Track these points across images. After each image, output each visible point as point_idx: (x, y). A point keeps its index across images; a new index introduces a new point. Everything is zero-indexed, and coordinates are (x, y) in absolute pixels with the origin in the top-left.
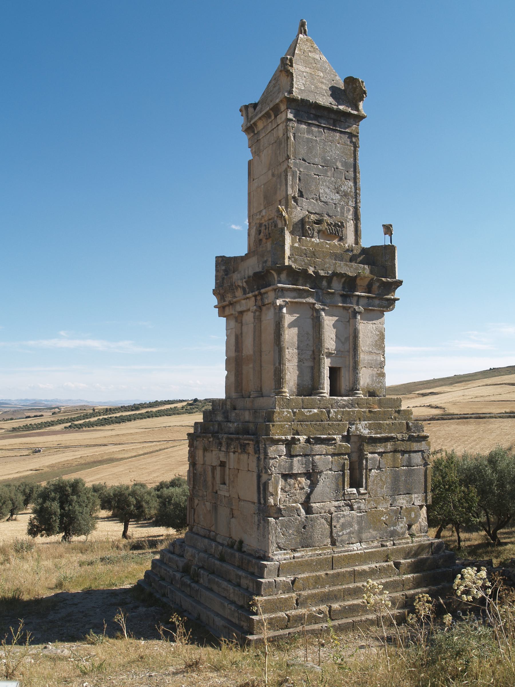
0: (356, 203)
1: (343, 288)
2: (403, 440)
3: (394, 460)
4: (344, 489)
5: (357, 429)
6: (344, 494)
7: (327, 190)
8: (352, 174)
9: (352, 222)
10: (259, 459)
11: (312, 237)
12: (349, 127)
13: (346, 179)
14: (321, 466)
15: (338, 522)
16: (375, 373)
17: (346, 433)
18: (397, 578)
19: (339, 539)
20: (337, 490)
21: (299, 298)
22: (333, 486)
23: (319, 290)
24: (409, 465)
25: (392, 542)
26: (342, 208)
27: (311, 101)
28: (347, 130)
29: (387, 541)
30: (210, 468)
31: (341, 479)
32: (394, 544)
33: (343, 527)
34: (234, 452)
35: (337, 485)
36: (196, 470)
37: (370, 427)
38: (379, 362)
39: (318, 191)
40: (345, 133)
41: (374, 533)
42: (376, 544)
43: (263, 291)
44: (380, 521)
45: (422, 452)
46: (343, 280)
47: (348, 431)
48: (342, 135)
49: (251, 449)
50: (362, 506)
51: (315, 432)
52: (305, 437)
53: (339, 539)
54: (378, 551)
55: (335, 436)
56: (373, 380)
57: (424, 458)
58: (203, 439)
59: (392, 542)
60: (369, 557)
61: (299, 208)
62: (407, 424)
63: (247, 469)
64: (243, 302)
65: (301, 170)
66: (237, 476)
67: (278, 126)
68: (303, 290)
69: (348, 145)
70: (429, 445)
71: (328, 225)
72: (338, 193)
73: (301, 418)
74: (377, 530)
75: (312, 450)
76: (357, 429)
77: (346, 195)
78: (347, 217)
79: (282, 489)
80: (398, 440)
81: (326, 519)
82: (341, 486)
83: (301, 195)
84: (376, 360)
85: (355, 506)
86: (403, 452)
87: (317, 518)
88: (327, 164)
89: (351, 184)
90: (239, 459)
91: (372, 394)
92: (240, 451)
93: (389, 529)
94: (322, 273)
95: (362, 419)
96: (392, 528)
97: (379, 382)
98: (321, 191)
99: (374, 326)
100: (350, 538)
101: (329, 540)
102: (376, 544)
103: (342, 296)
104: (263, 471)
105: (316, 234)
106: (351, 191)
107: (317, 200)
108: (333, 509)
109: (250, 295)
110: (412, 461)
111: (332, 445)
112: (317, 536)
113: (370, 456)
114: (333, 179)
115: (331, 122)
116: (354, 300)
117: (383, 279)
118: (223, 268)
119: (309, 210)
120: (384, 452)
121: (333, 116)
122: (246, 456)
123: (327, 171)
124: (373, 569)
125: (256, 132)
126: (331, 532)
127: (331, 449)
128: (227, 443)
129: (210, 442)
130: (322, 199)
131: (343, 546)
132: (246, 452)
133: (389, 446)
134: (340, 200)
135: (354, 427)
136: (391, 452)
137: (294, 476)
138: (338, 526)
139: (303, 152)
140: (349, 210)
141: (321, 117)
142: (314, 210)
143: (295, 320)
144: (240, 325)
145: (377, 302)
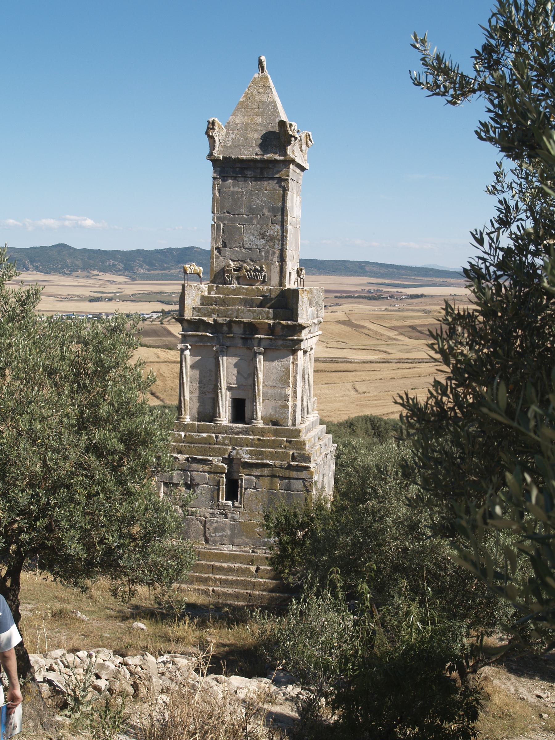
0: (282, 245)
1: (245, 332)
2: (281, 468)
3: (272, 483)
4: (218, 501)
5: (237, 453)
6: (218, 505)
7: (252, 238)
8: (279, 217)
9: (277, 263)
11: (230, 284)
12: (278, 172)
13: (272, 223)
14: (197, 480)
15: (211, 525)
16: (278, 405)
17: (226, 456)
18: (252, 580)
19: (212, 539)
20: (212, 500)
21: (201, 342)
22: (209, 496)
23: (220, 335)
24: (288, 488)
25: (264, 551)
26: (268, 252)
27: (233, 157)
28: (277, 176)
29: (259, 549)
31: (216, 493)
32: (265, 553)
33: (216, 530)
35: (213, 497)
37: (251, 453)
38: (283, 396)
39: (242, 239)
40: (273, 179)
41: (247, 540)
42: (247, 549)
44: (253, 531)
45: (304, 480)
46: (242, 325)
47: (229, 455)
48: (270, 182)
50: (236, 517)
51: (197, 453)
52: (187, 456)
53: (212, 539)
54: (243, 555)
55: (211, 458)
56: (276, 411)
57: (305, 486)
59: (264, 551)
60: (234, 558)
61: (222, 258)
62: (293, 454)
65: (225, 222)
68: (202, 335)
69: (276, 190)
70: (311, 474)
71: (247, 271)
72: (263, 238)
73: (190, 441)
74: (250, 538)
75: (189, 467)
76: (237, 453)
77: (272, 238)
78: (272, 260)
79: (164, 493)
80: (276, 467)
81: (201, 522)
82: (216, 498)
83: (225, 245)
84: (280, 394)
85: (230, 516)
86: (282, 478)
87: (192, 519)
88: (252, 212)
89: (278, 227)
91: (275, 423)
93: (262, 540)
94: (220, 320)
95: (249, 445)
96: (266, 540)
97: (282, 413)
98: (245, 239)
99: (280, 363)
100: (222, 540)
101: (203, 538)
102: (247, 549)
103: (242, 338)
105: (234, 281)
106: (277, 235)
107: (240, 247)
108: (207, 515)
110: (292, 486)
111: (209, 464)
112: (193, 532)
113: (245, 477)
114: (258, 226)
115: (259, 171)
116: (256, 342)
117: (283, 322)
119: (232, 258)
120: (261, 476)
121: (260, 165)
123: (252, 219)
124: (231, 567)
126: (205, 532)
127: (207, 468)
130: (246, 246)
131: (215, 545)
133: (266, 471)
134: (265, 245)
135: (235, 451)
136: (268, 476)
137: (176, 485)
138: (211, 529)
139: (227, 205)
140: (275, 253)
141: (247, 169)
142: (237, 257)
143: (199, 360)
145: (280, 342)
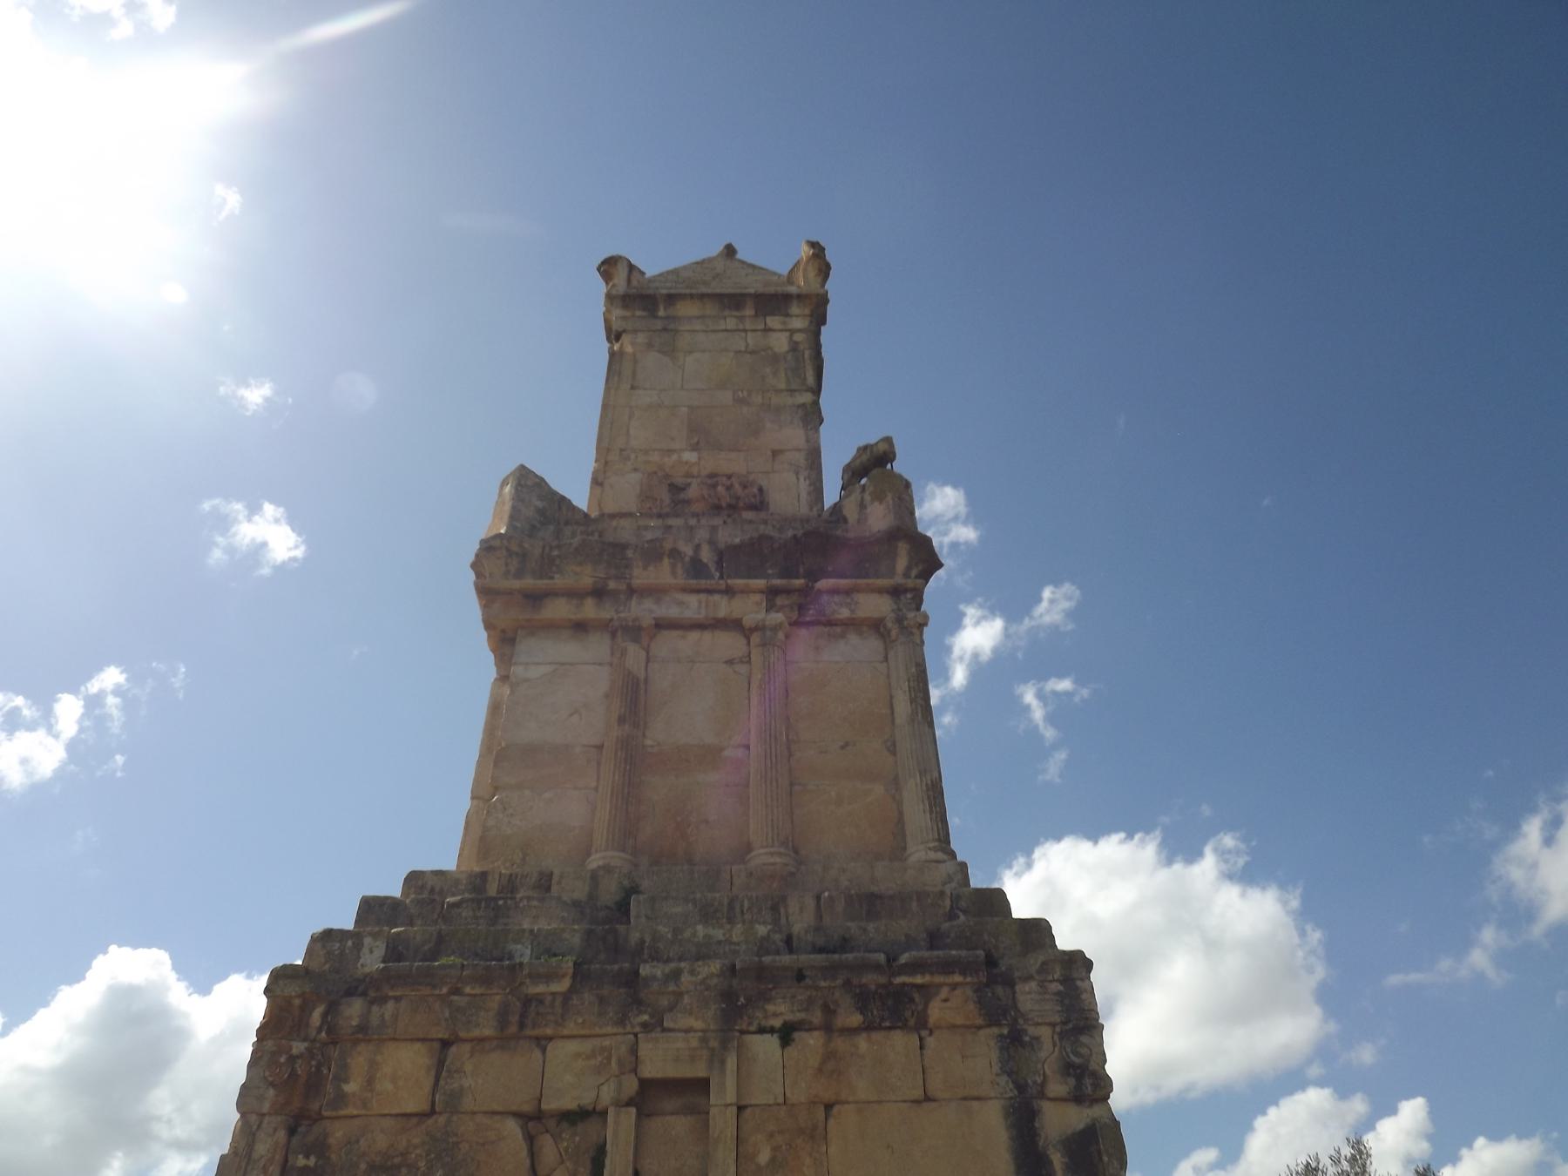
10: (1015, 1042)
30: (512, 1127)
34: (786, 1035)
36: (319, 1148)
43: (823, 584)
49: (950, 1005)
58: (456, 991)
63: (918, 1093)
64: (693, 600)
66: (816, 1135)
67: (767, 330)
90: (829, 1055)
92: (856, 1019)
104: (1057, 1088)
109: (760, 583)
118: (539, 504)
122: (900, 1043)
125: (661, 313)
128: (728, 996)
129: (527, 1001)
132: (904, 1027)
144: (643, 654)
